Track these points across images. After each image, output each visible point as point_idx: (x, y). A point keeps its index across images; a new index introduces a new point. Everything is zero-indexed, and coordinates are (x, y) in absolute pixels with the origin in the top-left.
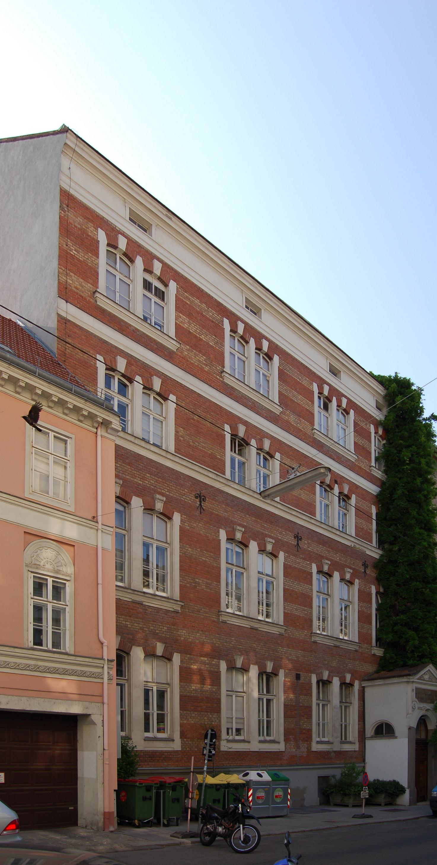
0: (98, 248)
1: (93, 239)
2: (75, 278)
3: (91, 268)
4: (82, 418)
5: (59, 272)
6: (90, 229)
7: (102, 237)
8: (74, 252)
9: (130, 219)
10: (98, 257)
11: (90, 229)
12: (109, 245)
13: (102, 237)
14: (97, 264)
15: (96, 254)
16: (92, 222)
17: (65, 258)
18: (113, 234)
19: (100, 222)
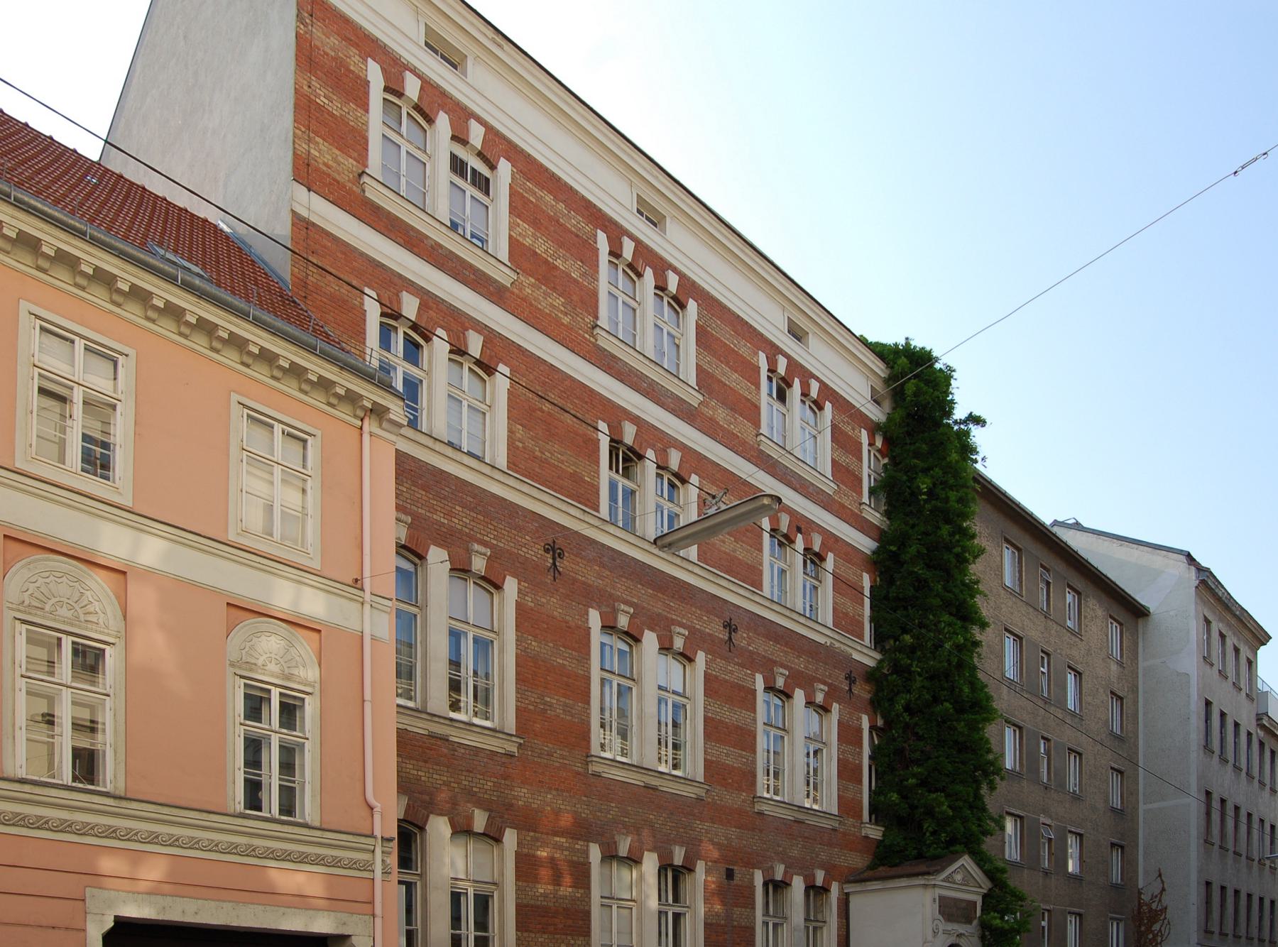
0: (367, 94)
1: (359, 77)
2: (324, 146)
3: (353, 129)
4: (277, 373)
5: (295, 135)
6: (354, 59)
7: (375, 74)
8: (322, 100)
9: (427, 44)
10: (367, 111)
11: (354, 59)
12: (386, 89)
13: (375, 74)
14: (366, 124)
15: (365, 107)
16: (357, 46)
17: (307, 112)
18: (395, 68)
19: (371, 46)
